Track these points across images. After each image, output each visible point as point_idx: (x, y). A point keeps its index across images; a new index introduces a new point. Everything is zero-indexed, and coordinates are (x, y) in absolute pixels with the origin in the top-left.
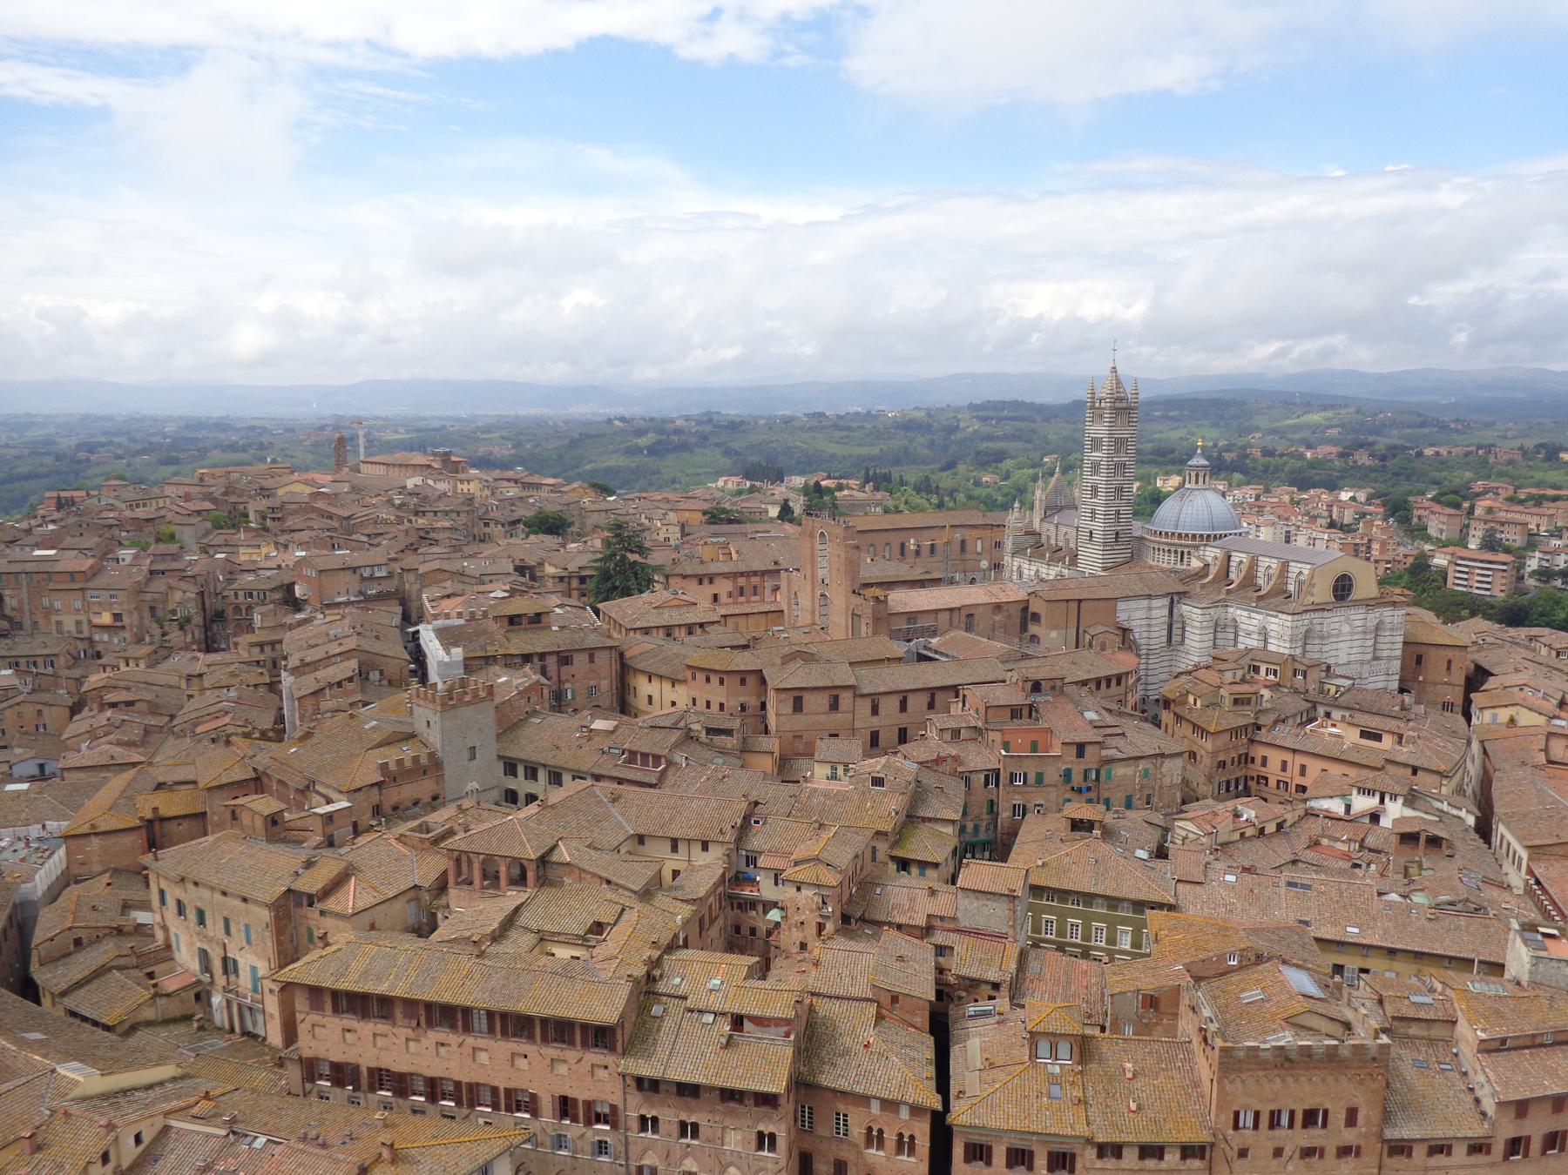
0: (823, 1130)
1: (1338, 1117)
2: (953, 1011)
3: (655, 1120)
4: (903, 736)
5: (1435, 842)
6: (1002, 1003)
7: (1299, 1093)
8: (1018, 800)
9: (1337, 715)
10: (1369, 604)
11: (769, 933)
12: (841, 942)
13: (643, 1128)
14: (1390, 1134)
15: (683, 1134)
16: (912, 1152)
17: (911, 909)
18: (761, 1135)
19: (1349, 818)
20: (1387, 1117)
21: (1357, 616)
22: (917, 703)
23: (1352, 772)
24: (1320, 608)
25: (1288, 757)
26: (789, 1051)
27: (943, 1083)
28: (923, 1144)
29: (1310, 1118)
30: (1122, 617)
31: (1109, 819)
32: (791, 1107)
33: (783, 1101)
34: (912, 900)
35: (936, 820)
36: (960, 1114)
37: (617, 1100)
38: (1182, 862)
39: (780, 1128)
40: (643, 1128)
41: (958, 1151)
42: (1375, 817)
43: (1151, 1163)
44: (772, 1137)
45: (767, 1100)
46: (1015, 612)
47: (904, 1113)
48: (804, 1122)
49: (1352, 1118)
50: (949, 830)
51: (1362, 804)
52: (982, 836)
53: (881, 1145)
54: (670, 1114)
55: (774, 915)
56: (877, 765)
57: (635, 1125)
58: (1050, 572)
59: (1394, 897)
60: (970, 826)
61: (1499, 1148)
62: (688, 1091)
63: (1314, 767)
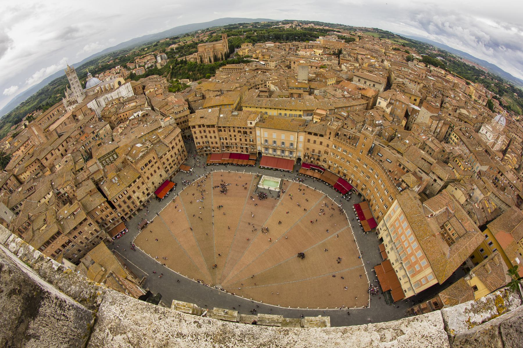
0: (95, 216)
1: (152, 159)
2: (100, 186)
3: (75, 236)
4: (66, 151)
5: (147, 114)
6: (105, 179)
7: (146, 160)
8: (89, 148)
9: (127, 103)
10: (124, 84)
11: (68, 198)
12: (78, 190)
13: (75, 238)
14: (159, 157)
15: (80, 234)
16: (108, 208)
17: (84, 176)
18: (89, 224)
19: (135, 118)
20: (158, 155)
21: (123, 86)
22: (65, 144)
23: (132, 111)
24: (118, 88)
25: (123, 114)
26: (83, 211)
27: (105, 196)
28: (109, 206)
29: (150, 162)
30: (89, 107)
31: (103, 141)
32: (89, 217)
33: (87, 218)
34: (83, 175)
35: (79, 160)
36: (110, 198)
37: (68, 239)
38: (116, 139)
39: (90, 221)
40: (75, 238)
41: (113, 203)
42: (138, 116)
43: (136, 183)
44: (90, 223)
45: (85, 220)
46: (71, 117)
47: (103, 204)
48: (92, 217)
49: (154, 158)
50: (81, 160)
51: (135, 115)
52: (87, 157)
53: (104, 211)
54: (76, 233)
55: (66, 195)
56: (65, 159)
57: (74, 239)
58: (74, 106)
59: (145, 125)
60: (85, 157)
61: (171, 149)
62: (75, 228)
63: (127, 113)
